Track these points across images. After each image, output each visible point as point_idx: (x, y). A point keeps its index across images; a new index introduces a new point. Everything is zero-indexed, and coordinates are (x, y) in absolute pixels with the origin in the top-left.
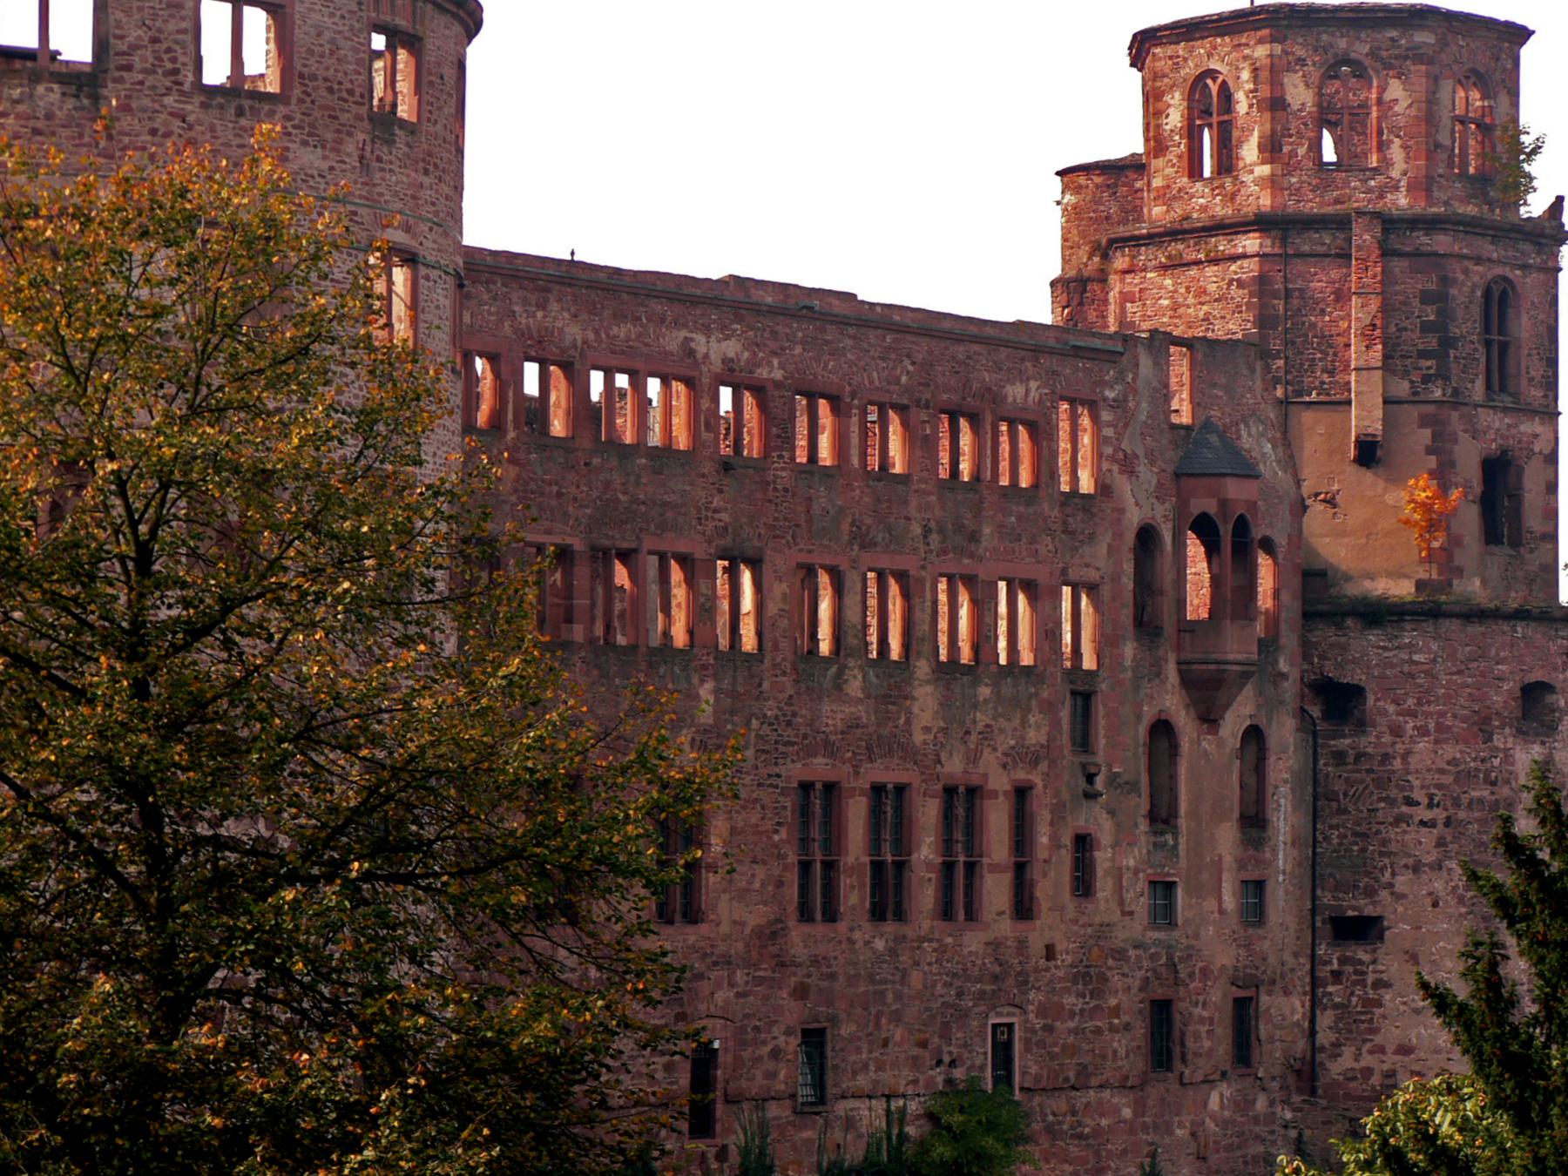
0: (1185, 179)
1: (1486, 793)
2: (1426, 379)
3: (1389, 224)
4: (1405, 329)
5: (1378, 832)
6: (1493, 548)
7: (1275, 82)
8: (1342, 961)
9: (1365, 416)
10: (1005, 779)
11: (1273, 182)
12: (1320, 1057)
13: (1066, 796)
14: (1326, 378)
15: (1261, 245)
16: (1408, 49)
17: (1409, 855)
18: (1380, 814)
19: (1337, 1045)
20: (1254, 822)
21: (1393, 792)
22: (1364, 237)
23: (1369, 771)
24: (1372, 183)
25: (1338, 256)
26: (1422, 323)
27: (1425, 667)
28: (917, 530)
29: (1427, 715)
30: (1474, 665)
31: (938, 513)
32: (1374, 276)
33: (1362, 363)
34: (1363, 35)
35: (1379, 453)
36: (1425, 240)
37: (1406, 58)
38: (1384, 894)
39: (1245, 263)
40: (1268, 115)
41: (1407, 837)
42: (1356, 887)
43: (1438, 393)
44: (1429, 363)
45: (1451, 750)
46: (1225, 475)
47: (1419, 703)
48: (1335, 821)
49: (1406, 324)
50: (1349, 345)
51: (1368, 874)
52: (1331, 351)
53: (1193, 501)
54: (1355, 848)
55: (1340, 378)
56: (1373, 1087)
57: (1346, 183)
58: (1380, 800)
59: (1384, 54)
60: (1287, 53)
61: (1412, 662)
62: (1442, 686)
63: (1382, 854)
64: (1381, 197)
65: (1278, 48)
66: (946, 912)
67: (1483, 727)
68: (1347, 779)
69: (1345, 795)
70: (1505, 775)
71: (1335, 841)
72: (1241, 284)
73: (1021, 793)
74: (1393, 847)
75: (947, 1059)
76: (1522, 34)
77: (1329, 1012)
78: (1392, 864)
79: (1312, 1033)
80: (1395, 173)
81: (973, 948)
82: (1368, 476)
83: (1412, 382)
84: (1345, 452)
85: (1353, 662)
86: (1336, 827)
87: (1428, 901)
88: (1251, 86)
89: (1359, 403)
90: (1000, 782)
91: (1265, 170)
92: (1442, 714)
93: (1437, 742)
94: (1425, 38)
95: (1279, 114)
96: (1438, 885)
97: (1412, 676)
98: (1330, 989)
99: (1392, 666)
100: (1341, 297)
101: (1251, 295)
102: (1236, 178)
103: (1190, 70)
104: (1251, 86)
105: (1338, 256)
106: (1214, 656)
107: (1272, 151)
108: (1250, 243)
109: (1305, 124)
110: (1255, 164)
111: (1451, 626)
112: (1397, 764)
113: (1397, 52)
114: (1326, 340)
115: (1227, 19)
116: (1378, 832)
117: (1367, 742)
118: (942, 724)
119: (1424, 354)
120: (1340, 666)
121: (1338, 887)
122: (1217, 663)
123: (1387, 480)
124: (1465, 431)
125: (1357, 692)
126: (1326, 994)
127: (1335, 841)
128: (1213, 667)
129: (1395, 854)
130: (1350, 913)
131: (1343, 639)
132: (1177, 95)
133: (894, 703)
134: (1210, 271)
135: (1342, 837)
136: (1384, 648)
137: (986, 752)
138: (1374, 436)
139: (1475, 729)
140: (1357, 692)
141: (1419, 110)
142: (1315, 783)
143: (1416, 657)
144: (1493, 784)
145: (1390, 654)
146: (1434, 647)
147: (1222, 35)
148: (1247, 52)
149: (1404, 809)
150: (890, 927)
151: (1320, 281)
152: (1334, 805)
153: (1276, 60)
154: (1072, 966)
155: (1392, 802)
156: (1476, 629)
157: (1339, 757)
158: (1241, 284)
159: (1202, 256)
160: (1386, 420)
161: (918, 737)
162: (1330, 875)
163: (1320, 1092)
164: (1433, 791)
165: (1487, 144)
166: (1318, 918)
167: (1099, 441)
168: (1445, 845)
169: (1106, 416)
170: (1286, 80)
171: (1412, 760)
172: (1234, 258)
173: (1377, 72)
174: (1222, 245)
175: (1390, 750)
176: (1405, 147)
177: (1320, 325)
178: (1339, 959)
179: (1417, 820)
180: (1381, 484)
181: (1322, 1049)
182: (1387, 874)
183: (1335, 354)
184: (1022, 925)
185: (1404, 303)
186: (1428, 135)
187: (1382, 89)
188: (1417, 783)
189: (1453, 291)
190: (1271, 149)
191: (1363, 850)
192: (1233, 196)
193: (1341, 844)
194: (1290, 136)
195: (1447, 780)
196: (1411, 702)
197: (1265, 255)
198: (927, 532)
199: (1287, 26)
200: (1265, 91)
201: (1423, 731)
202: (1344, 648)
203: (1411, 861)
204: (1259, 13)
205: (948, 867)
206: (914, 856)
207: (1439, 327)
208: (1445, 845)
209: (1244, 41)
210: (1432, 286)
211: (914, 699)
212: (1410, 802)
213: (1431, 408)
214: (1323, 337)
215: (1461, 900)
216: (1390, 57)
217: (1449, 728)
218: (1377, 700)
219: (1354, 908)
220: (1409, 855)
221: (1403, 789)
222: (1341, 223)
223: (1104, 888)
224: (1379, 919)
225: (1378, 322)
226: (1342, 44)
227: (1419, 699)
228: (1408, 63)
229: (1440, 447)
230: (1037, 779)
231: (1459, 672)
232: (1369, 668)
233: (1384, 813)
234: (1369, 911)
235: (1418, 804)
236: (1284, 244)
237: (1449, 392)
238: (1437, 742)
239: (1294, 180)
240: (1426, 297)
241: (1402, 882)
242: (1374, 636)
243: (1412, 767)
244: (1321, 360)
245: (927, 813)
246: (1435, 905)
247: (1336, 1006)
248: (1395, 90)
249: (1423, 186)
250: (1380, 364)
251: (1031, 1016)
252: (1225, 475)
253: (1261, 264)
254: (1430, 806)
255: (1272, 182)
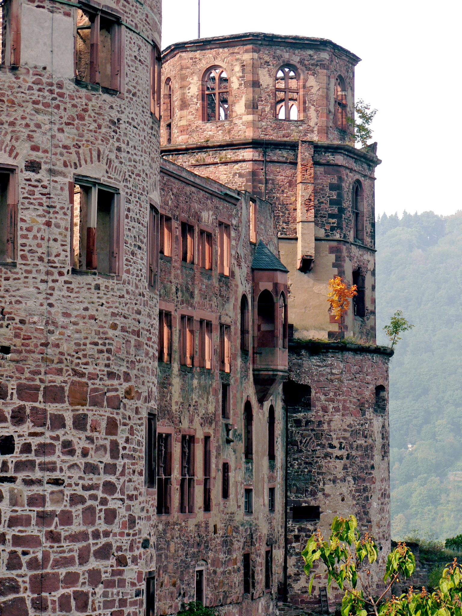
0: (201, 122)
1: (363, 442)
2: (332, 229)
3: (317, 148)
4: (322, 203)
5: (317, 462)
6: (357, 317)
7: (254, 73)
8: (299, 531)
9: (302, 247)
10: (202, 433)
11: (254, 124)
12: (289, 581)
13: (220, 442)
14: (284, 225)
15: (253, 156)
16: (318, 61)
17: (331, 474)
18: (318, 452)
19: (297, 574)
20: (272, 456)
21: (324, 441)
22: (304, 154)
23: (312, 430)
24: (301, 128)
25: (291, 163)
26: (330, 200)
27: (338, 376)
28: (174, 289)
29: (339, 401)
30: (357, 376)
31: (181, 280)
32: (310, 174)
33: (304, 219)
34: (296, 52)
35: (312, 265)
36: (331, 157)
37: (317, 65)
38: (320, 494)
39: (244, 164)
40: (251, 89)
41: (330, 464)
42: (307, 491)
43: (337, 237)
44: (334, 221)
45: (349, 420)
46: (276, 270)
47: (335, 395)
48: (296, 456)
49: (323, 200)
50: (295, 210)
51: (312, 484)
52: (287, 212)
53: (261, 284)
54: (306, 470)
55: (291, 226)
56: (315, 596)
57: (289, 127)
58: (318, 445)
59: (306, 62)
60: (260, 59)
61: (332, 374)
62: (345, 387)
63: (318, 474)
64: (305, 135)
65: (256, 55)
66: (182, 509)
67: (361, 408)
68: (302, 434)
69: (301, 442)
70: (370, 433)
71: (296, 467)
72: (241, 175)
73: (207, 438)
74: (324, 470)
75: (182, 592)
76: (354, 60)
77: (294, 557)
78: (323, 478)
79: (285, 568)
80: (312, 124)
81: (191, 529)
82: (305, 277)
83: (326, 230)
84: (295, 265)
85: (304, 373)
86: (296, 459)
87: (340, 498)
88: (241, 74)
89: (303, 240)
90: (200, 435)
91: (250, 118)
92: (345, 401)
93: (343, 415)
94: (325, 55)
95: (257, 89)
96: (344, 490)
97: (332, 381)
98: (294, 545)
99: (323, 375)
100: (292, 184)
101: (247, 181)
102: (231, 121)
103: (204, 65)
104: (241, 74)
105: (291, 163)
106: (272, 367)
107: (254, 108)
108: (248, 154)
109: (270, 96)
110: (244, 115)
111: (349, 355)
112: (325, 426)
113: (313, 62)
114: (285, 206)
115: (228, 39)
116: (317, 462)
117: (311, 415)
118: (182, 400)
119: (331, 216)
120: (298, 375)
121: (298, 491)
122: (273, 370)
123: (314, 280)
124: (347, 256)
125: (307, 389)
126: (291, 547)
127: (296, 467)
128: (271, 373)
129: (325, 473)
130: (304, 505)
131: (300, 361)
132: (196, 78)
133: (166, 388)
134: (222, 168)
135: (300, 464)
136: (319, 366)
137: (196, 416)
138: (311, 256)
139: (358, 409)
140: (307, 389)
141: (323, 92)
142: (287, 437)
143: (334, 371)
144: (366, 437)
145: (322, 369)
146: (342, 366)
147: (224, 47)
148: (238, 56)
149: (329, 450)
150: (164, 517)
151: (281, 175)
152: (296, 448)
153: (255, 62)
154: (222, 537)
155: (323, 446)
156: (359, 357)
157: (298, 423)
158: (241, 175)
159: (217, 160)
160: (317, 249)
161: (174, 408)
162: (294, 485)
163: (289, 599)
164: (342, 440)
165: (344, 114)
166: (288, 507)
167: (230, 247)
168: (347, 469)
169: (233, 234)
170: (260, 72)
171: (332, 424)
172: (236, 162)
173: (303, 72)
174: (230, 155)
175: (322, 419)
176: (317, 111)
177: (282, 198)
178: (298, 529)
179: (334, 455)
180: (312, 282)
181: (290, 576)
182: (321, 484)
183: (289, 214)
184: (207, 514)
185: (322, 189)
186: (327, 106)
187: (306, 80)
188: (334, 436)
189: (343, 185)
190: (253, 106)
191: (310, 471)
192: (229, 132)
193: (299, 468)
194: (262, 101)
195: (348, 435)
196: (332, 394)
197: (256, 161)
198: (177, 290)
199: (261, 44)
200: (249, 77)
201: (337, 409)
202: (300, 366)
203: (332, 477)
204: (248, 36)
205: (183, 480)
206: (172, 476)
207: (337, 202)
208: (347, 469)
209: (236, 51)
210: (335, 181)
211: (173, 385)
212: (332, 446)
213: (335, 244)
214: (283, 205)
215: (354, 497)
216: (309, 64)
217: (348, 408)
218: (316, 393)
219: (305, 502)
220: (331, 474)
221: (328, 439)
222: (293, 146)
223: (232, 495)
224: (318, 507)
225: (312, 198)
226: (286, 56)
227: (335, 393)
228: (318, 68)
229: (338, 264)
230: (211, 432)
231: (352, 379)
232: (312, 376)
233: (320, 452)
234: (313, 503)
235: (335, 447)
236: (265, 154)
237: (342, 236)
238: (343, 415)
239: (264, 124)
240: (332, 187)
241: (328, 488)
242: (315, 360)
243: (332, 428)
244: (282, 216)
245: (176, 450)
246: (343, 500)
247: (297, 554)
248: (312, 81)
249: (325, 131)
250: (313, 220)
251: (209, 565)
252: (276, 270)
253: (253, 165)
254: (341, 448)
255: (253, 124)
